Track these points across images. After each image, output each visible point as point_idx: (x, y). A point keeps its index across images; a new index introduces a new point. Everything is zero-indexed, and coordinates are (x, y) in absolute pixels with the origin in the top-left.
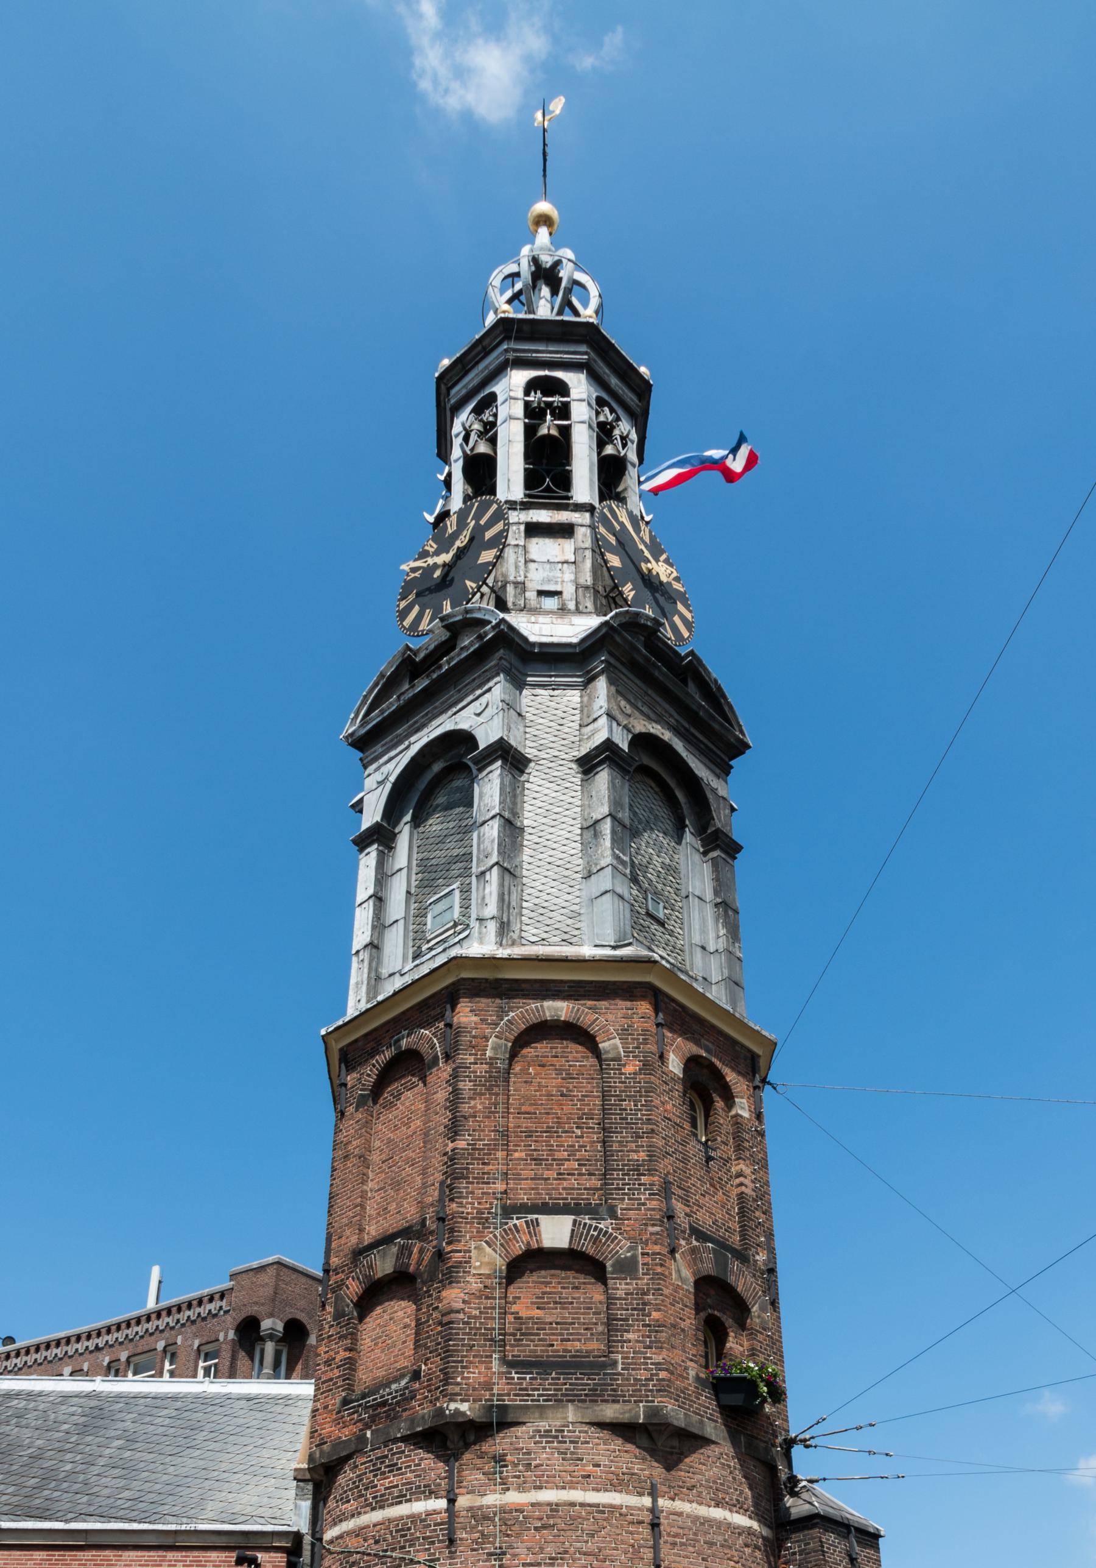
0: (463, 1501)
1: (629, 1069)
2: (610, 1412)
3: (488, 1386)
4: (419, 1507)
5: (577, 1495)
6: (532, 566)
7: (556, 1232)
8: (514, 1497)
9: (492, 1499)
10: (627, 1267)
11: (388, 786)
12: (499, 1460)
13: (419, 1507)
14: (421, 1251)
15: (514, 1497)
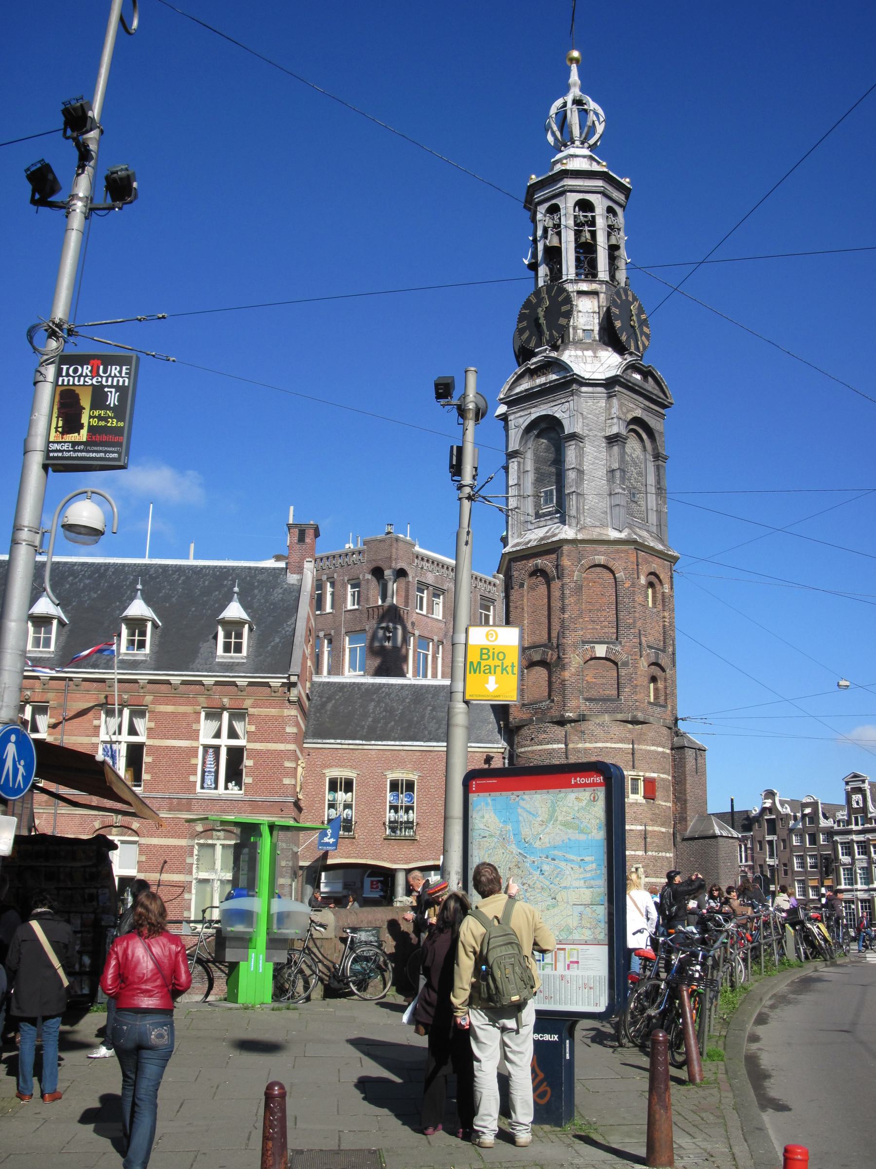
0: (571, 746)
1: (627, 585)
2: (620, 716)
3: (579, 707)
4: (555, 746)
5: (608, 745)
6: (580, 314)
7: (601, 651)
8: (588, 745)
9: (580, 746)
10: (625, 664)
11: (521, 431)
12: (583, 732)
13: (555, 746)
14: (552, 655)
15: (588, 745)
